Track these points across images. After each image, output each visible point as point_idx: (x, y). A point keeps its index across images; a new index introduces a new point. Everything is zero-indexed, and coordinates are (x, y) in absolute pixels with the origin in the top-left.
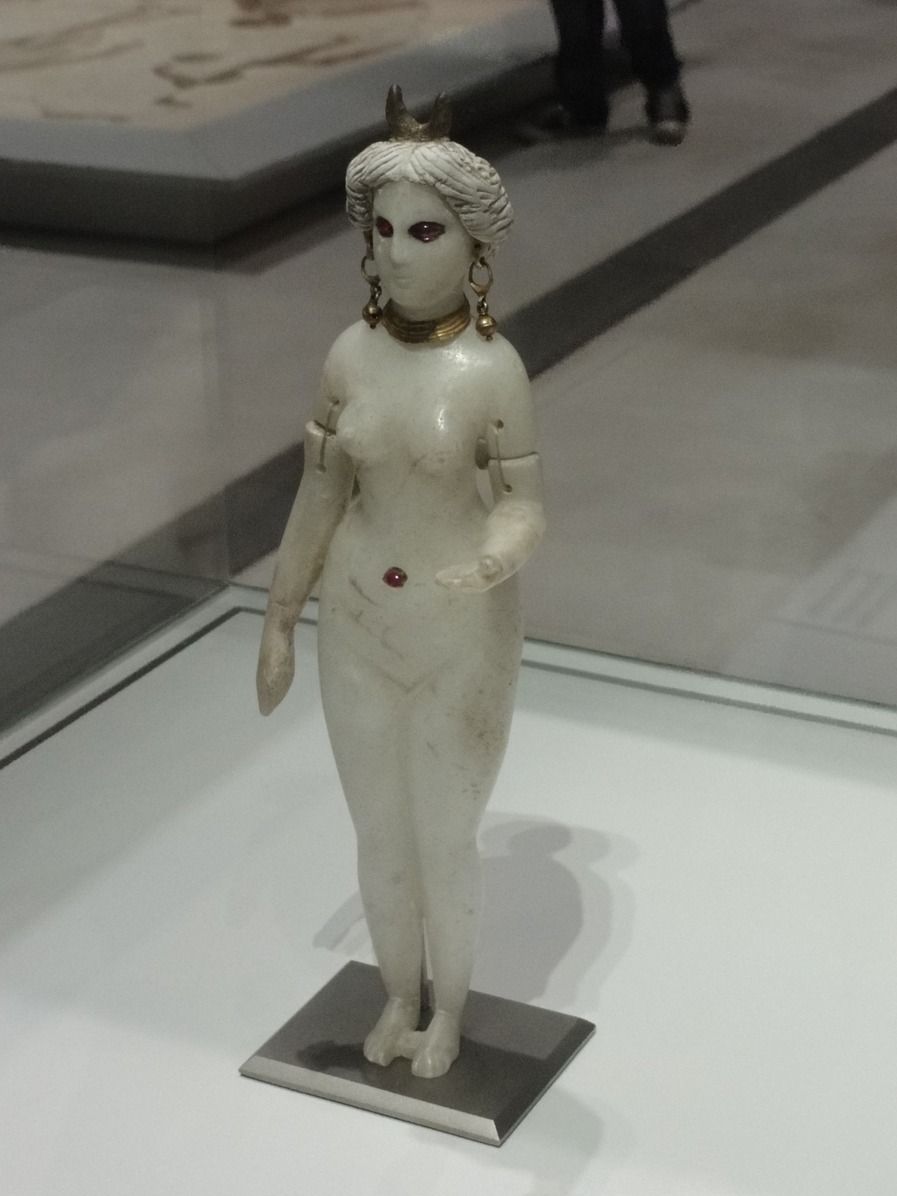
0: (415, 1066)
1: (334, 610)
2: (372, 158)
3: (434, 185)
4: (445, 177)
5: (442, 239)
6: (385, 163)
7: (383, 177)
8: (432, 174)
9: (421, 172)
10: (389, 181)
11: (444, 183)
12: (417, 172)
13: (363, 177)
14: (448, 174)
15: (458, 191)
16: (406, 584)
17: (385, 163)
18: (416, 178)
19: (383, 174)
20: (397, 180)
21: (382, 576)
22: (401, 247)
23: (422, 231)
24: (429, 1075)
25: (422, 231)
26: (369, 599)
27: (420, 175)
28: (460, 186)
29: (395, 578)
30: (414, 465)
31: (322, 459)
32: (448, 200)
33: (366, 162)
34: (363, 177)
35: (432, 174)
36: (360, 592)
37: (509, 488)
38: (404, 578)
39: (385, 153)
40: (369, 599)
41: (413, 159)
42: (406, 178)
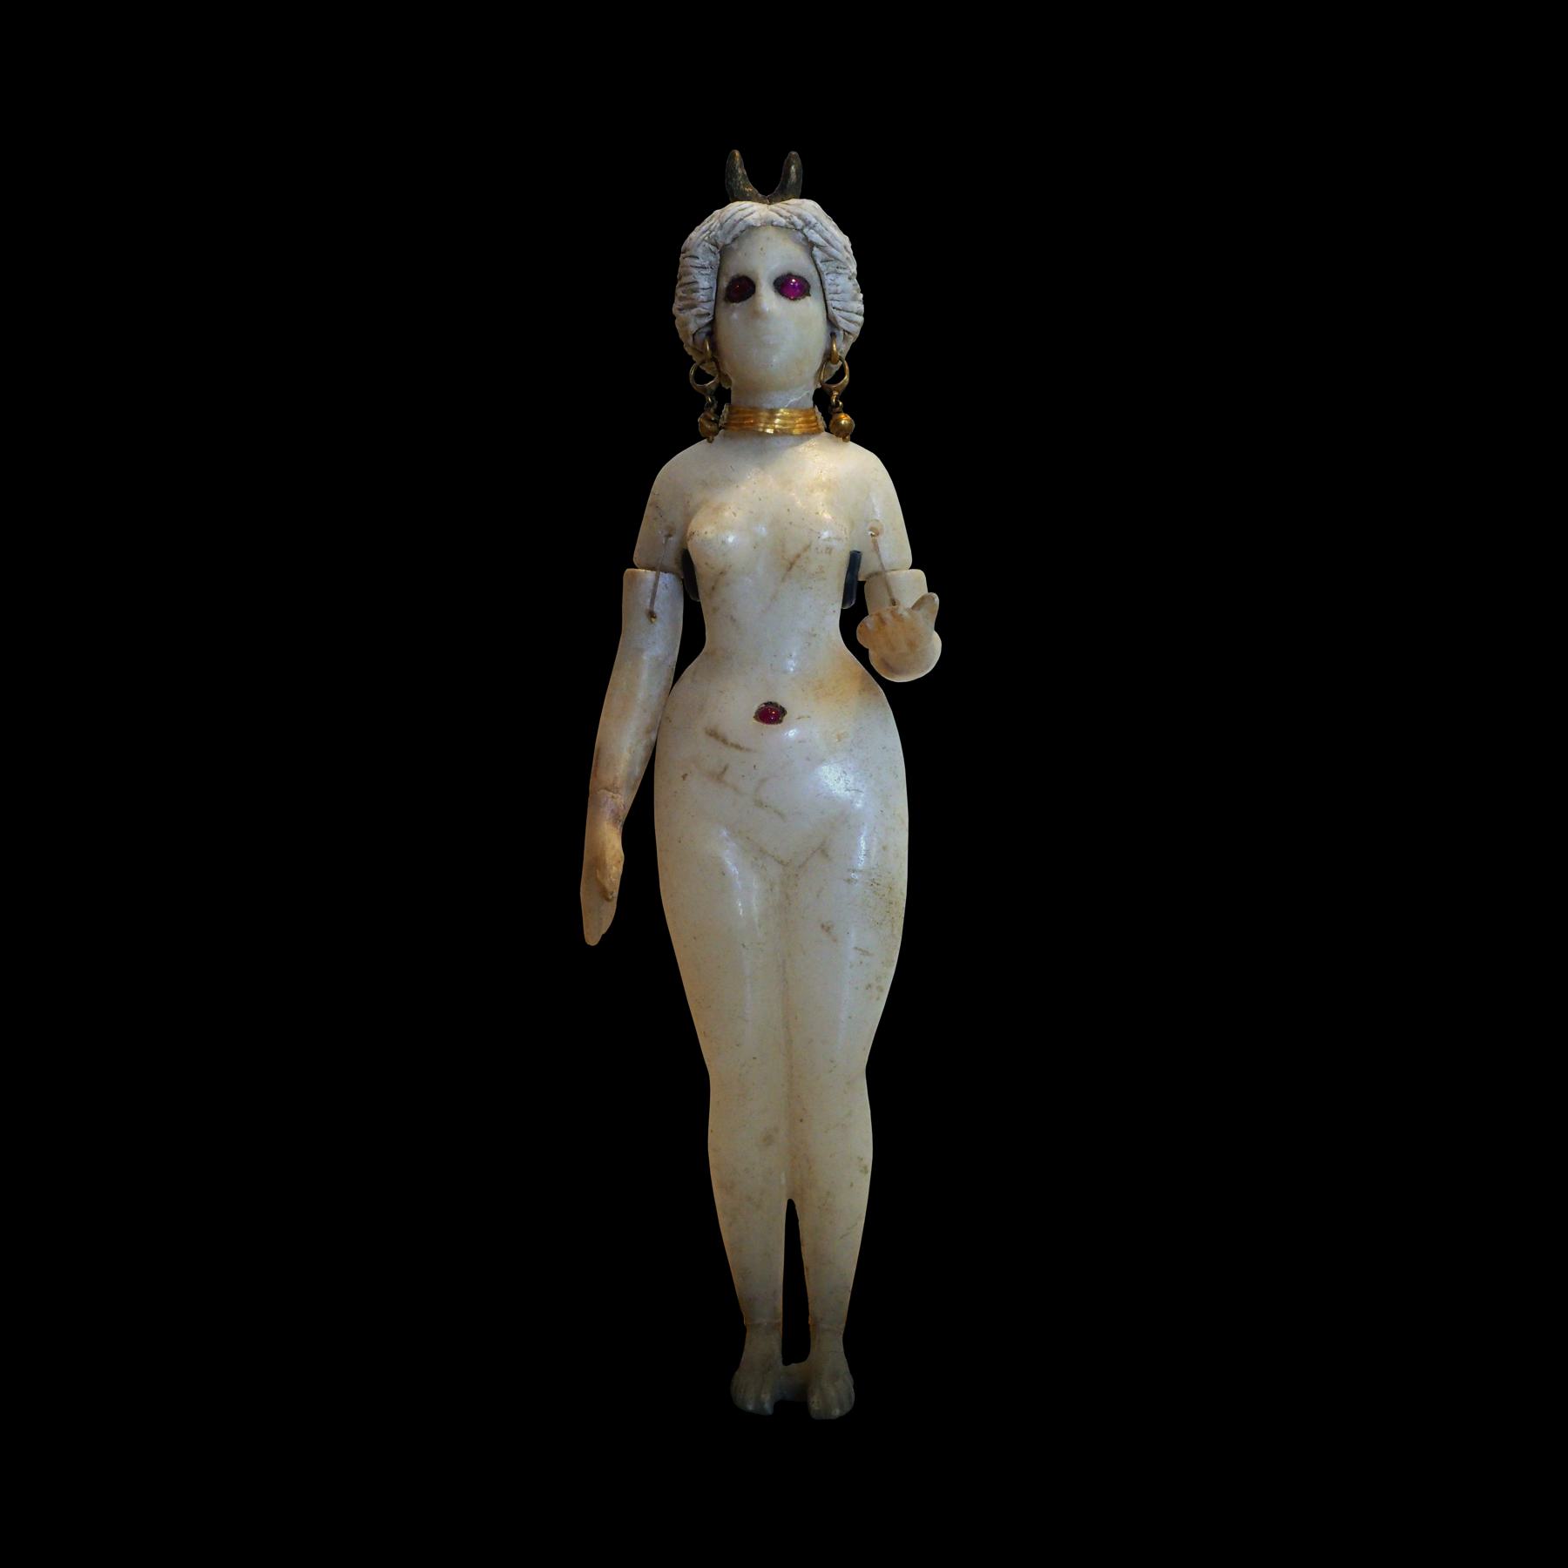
0: (815, 1405)
1: (684, 777)
3: (801, 230)
8: (799, 216)
10: (751, 228)
18: (783, 221)
24: (837, 1413)
25: (791, 287)
26: (737, 747)
28: (828, 236)
29: (771, 714)
30: (792, 564)
31: (652, 602)
35: (799, 216)
36: (724, 741)
38: (783, 712)
40: (737, 747)
42: (772, 223)
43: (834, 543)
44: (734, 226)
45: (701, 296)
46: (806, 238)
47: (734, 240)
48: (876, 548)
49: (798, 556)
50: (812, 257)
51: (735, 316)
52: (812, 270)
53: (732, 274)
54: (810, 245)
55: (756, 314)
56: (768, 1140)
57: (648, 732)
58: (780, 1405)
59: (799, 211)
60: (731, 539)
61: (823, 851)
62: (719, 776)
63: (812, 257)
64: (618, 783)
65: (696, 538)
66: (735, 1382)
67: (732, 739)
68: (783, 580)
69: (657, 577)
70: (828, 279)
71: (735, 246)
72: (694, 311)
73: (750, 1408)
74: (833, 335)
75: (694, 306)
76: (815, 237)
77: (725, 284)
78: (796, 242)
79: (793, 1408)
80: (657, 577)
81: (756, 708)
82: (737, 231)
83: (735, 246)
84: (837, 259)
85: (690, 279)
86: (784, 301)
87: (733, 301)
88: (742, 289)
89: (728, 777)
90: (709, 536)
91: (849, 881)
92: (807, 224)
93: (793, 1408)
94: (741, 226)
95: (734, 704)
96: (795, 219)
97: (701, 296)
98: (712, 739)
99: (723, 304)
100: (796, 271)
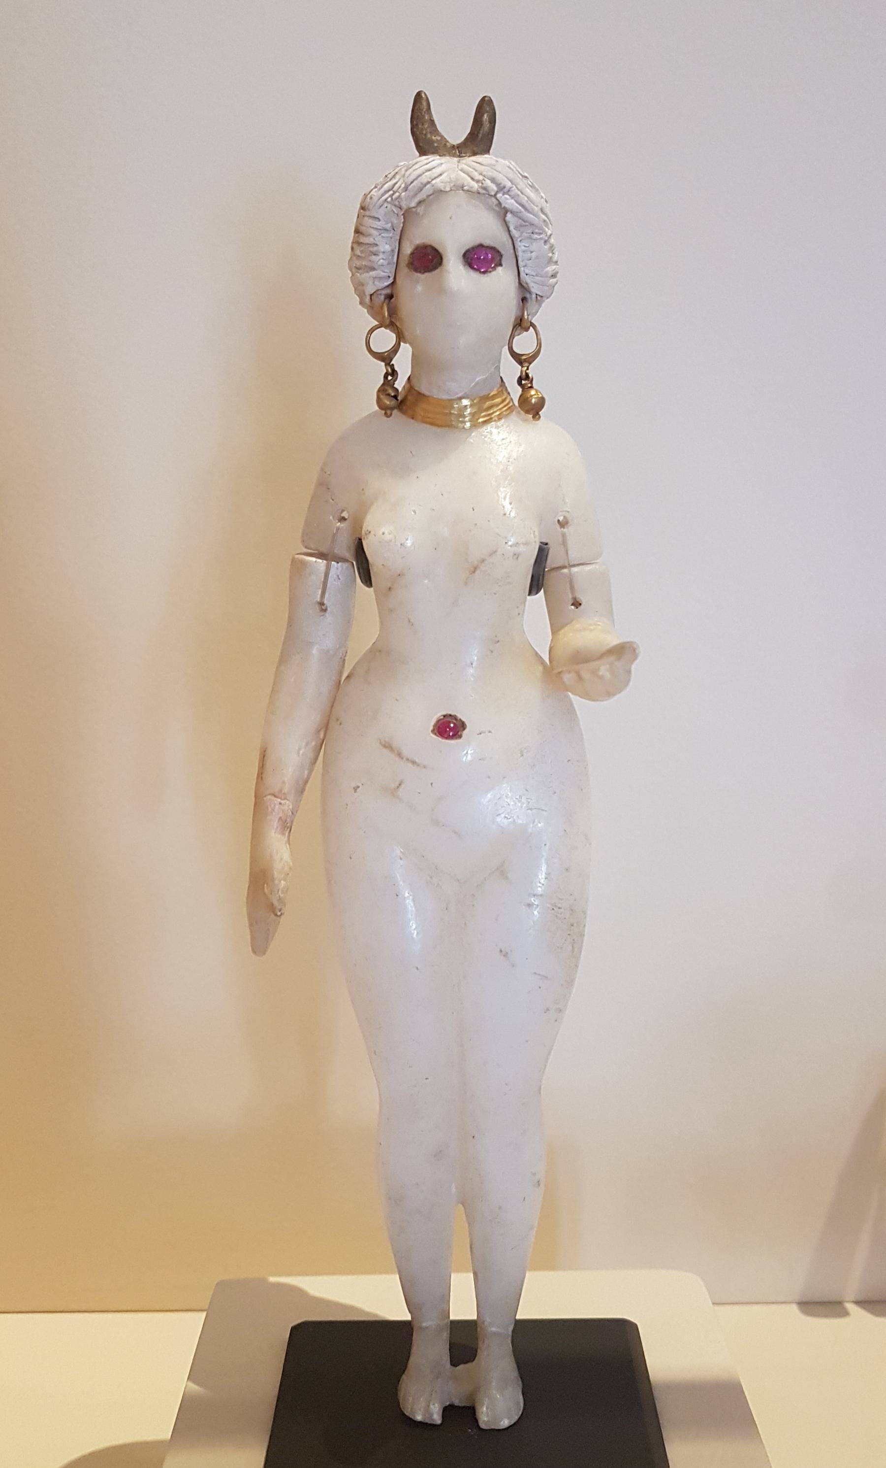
1: (356, 789)
2: (406, 170)
4: (509, 184)
5: (499, 269)
6: (429, 170)
7: (428, 186)
8: (493, 180)
9: (481, 178)
10: (439, 193)
11: (508, 192)
12: (472, 179)
13: (397, 194)
14: (511, 181)
15: (523, 206)
16: (465, 733)
17: (429, 170)
18: (476, 186)
19: (429, 183)
20: (448, 189)
21: (431, 728)
22: (456, 274)
23: (480, 258)
24: (505, 1423)
25: (480, 258)
26: (414, 762)
27: (478, 181)
28: (524, 200)
29: (449, 728)
30: (475, 569)
32: (509, 216)
33: (398, 177)
34: (397, 194)
35: (493, 180)
36: (400, 755)
37: (577, 604)
38: (463, 726)
39: (426, 161)
40: (414, 762)
41: (465, 167)
43: (522, 549)
44: (421, 189)
45: (380, 260)
46: (500, 204)
47: (420, 203)
48: (564, 543)
49: (483, 561)
50: (506, 224)
51: (419, 288)
52: (505, 238)
53: (418, 241)
54: (503, 212)
55: (441, 290)
56: (439, 1154)
57: (318, 731)
58: (449, 1411)
59: (491, 173)
60: (409, 543)
61: (502, 872)
62: (394, 791)
63: (506, 224)
64: (286, 790)
65: (371, 536)
66: (401, 1396)
67: (406, 752)
68: (466, 584)
69: (328, 568)
70: (521, 246)
71: (420, 210)
72: (373, 273)
73: (419, 1418)
74: (524, 300)
75: (374, 269)
76: (508, 202)
77: (408, 250)
78: (490, 208)
79: (461, 1415)
80: (328, 568)
81: (433, 721)
82: (422, 195)
83: (420, 210)
84: (532, 224)
85: (370, 240)
86: (474, 275)
87: (417, 270)
88: (428, 259)
89: (401, 792)
90: (388, 537)
91: (530, 905)
92: (501, 188)
93: (461, 1415)
94: (428, 190)
95: (410, 714)
96: (488, 183)
97: (380, 260)
98: (386, 751)
99: (404, 270)
100: (487, 242)
